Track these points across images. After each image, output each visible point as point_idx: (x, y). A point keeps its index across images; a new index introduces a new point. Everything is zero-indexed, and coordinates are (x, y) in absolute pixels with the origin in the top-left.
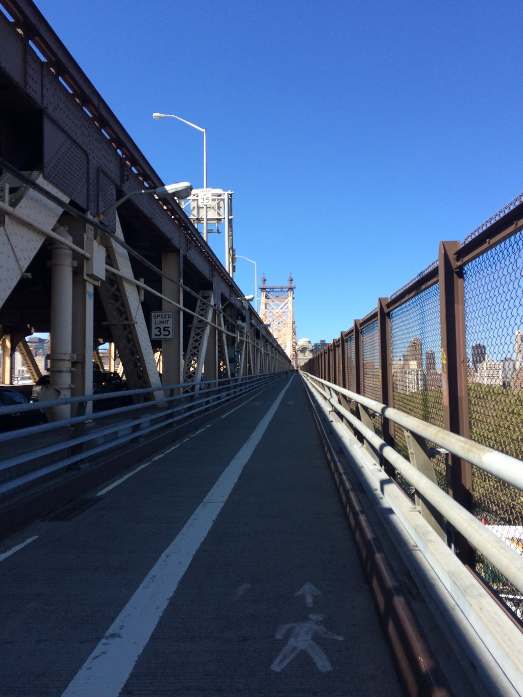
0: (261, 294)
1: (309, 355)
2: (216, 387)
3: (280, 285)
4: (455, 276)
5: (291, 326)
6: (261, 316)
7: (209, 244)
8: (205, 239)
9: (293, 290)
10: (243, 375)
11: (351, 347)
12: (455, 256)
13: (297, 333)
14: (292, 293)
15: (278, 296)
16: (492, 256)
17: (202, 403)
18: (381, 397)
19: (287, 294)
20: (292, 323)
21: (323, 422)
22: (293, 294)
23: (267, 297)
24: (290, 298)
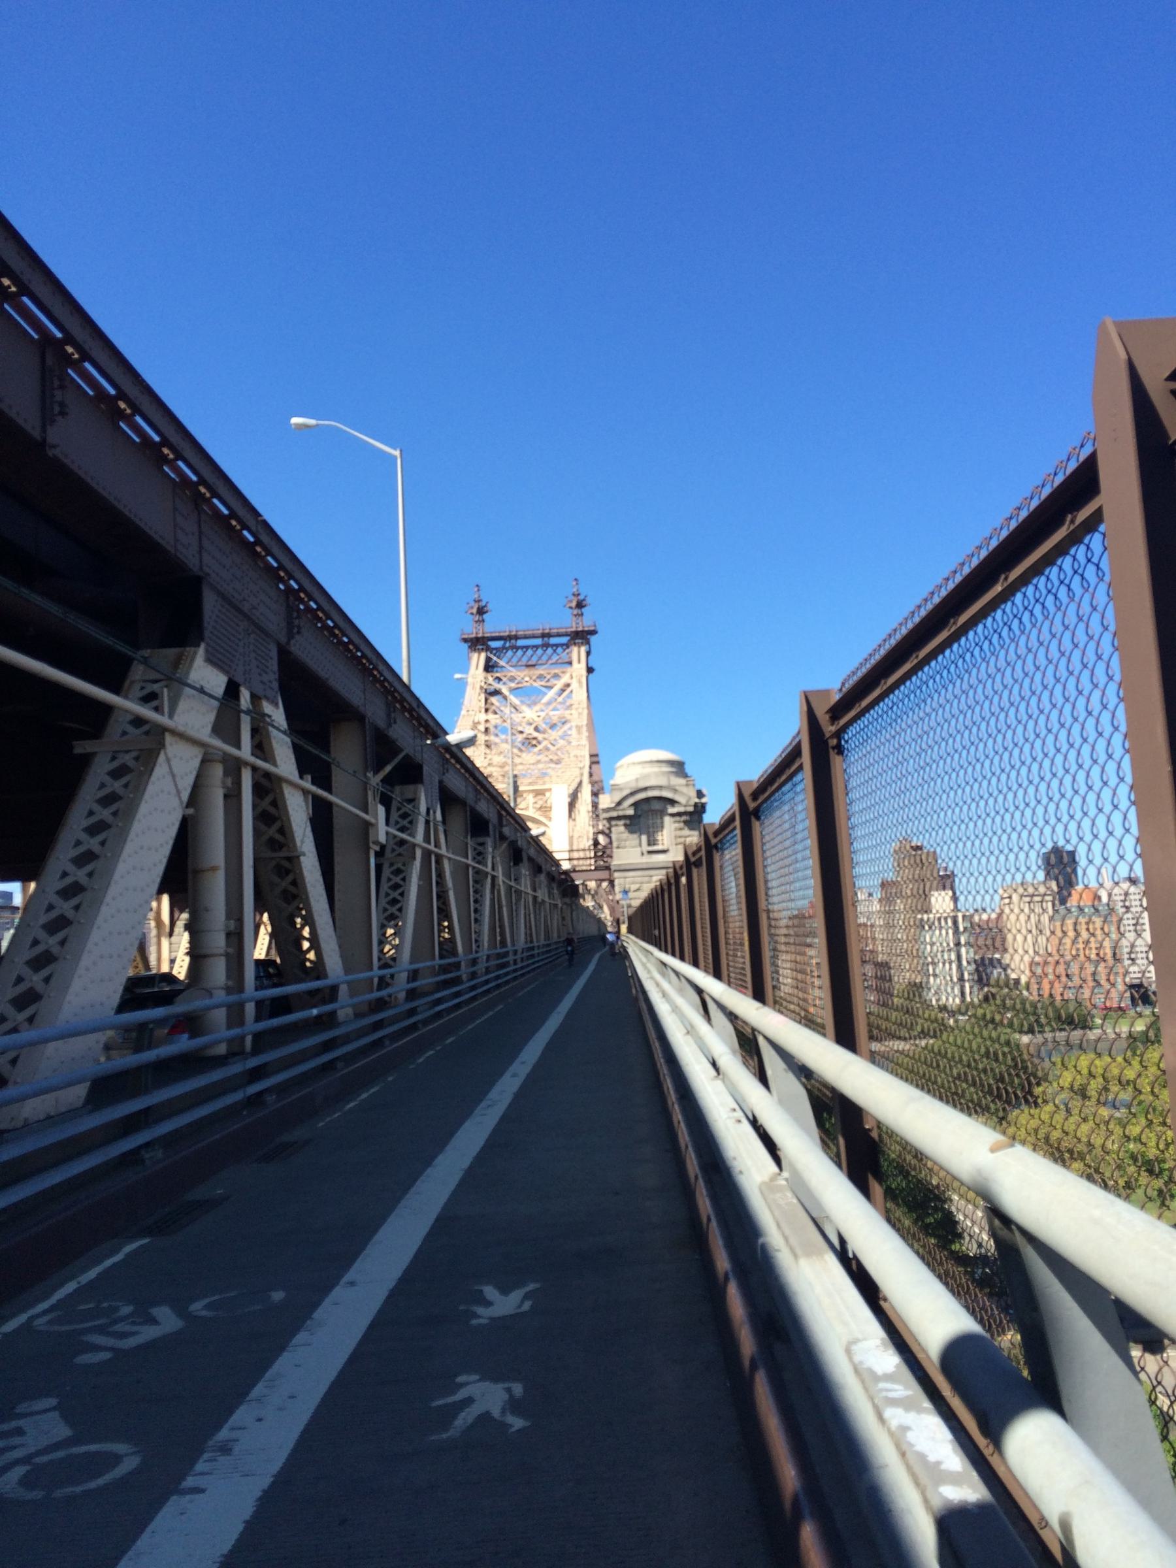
0: (469, 659)
9: (588, 643)
14: (583, 649)
19: (564, 656)
22: (588, 653)
23: (489, 667)
24: (579, 668)
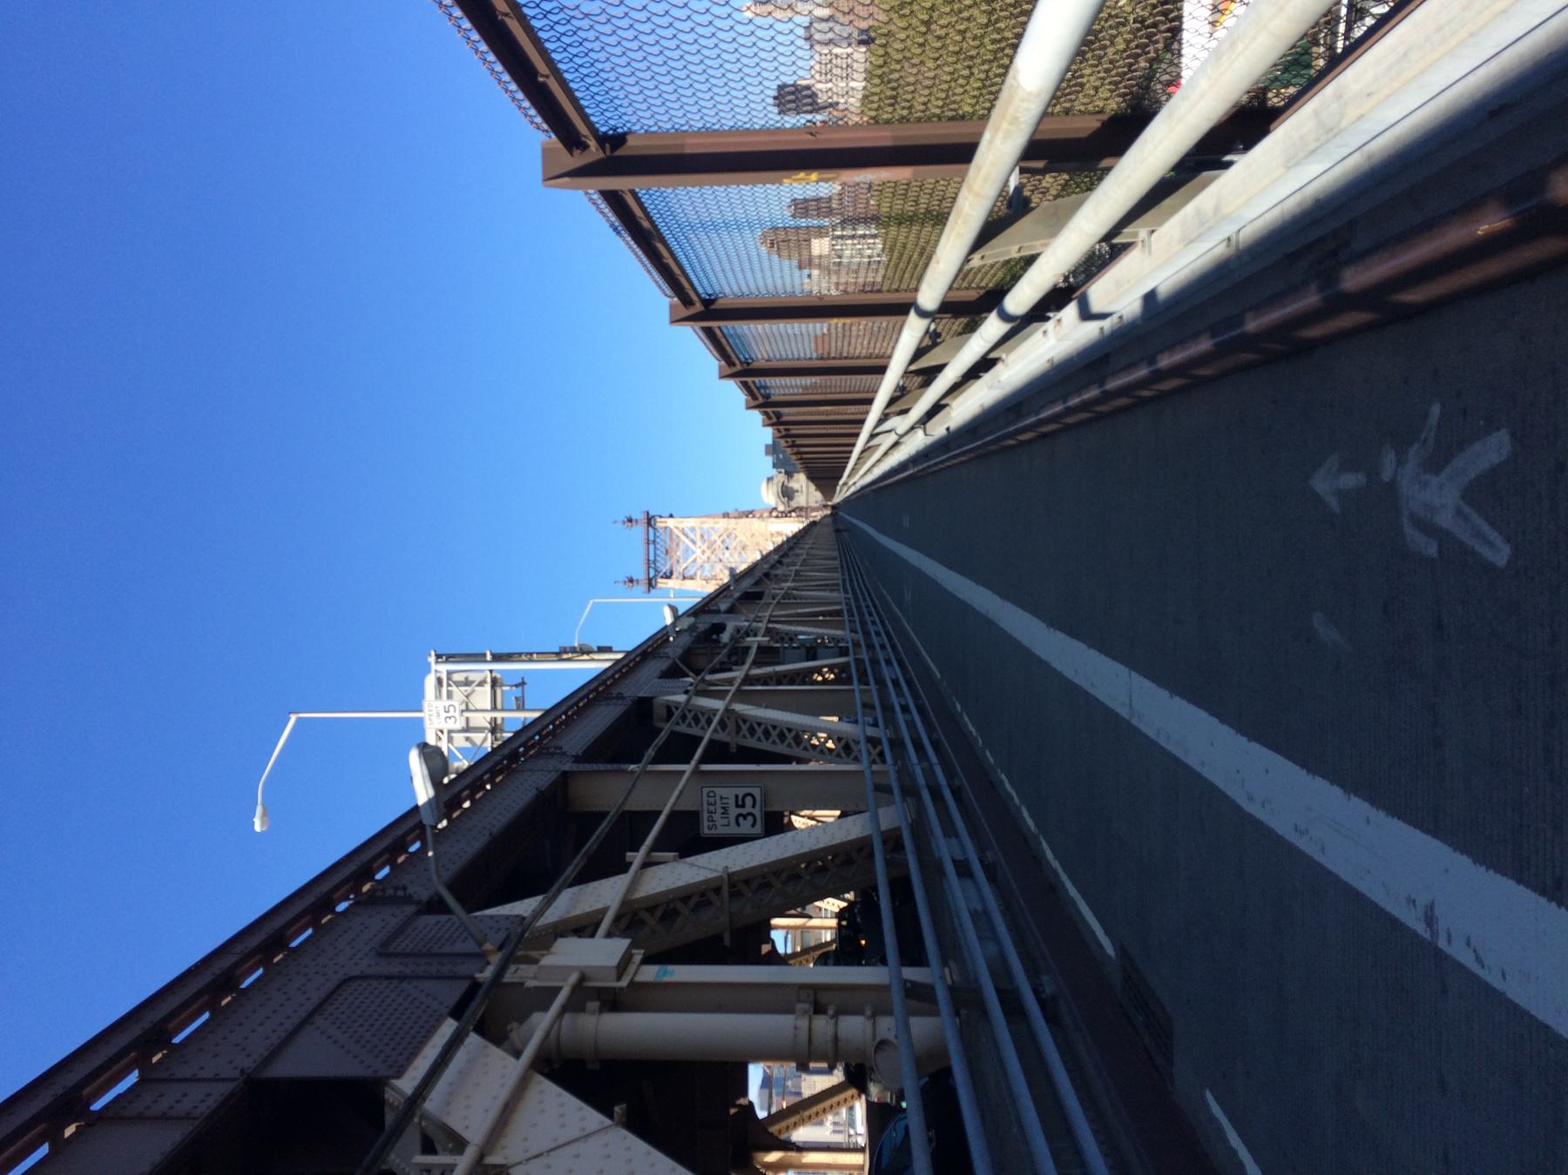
0: (661, 588)
1: (798, 481)
2: (870, 691)
3: (641, 547)
4: (620, 152)
5: (733, 521)
6: (711, 588)
7: (548, 706)
8: (537, 715)
9: (653, 517)
10: (844, 629)
11: (780, 387)
12: (577, 152)
13: (749, 508)
14: (658, 519)
15: (667, 551)
16: (577, 70)
17: (906, 722)
18: (893, 319)
19: (661, 531)
20: (726, 520)
21: (949, 451)
22: (661, 517)
23: (669, 576)
24: (671, 523)
